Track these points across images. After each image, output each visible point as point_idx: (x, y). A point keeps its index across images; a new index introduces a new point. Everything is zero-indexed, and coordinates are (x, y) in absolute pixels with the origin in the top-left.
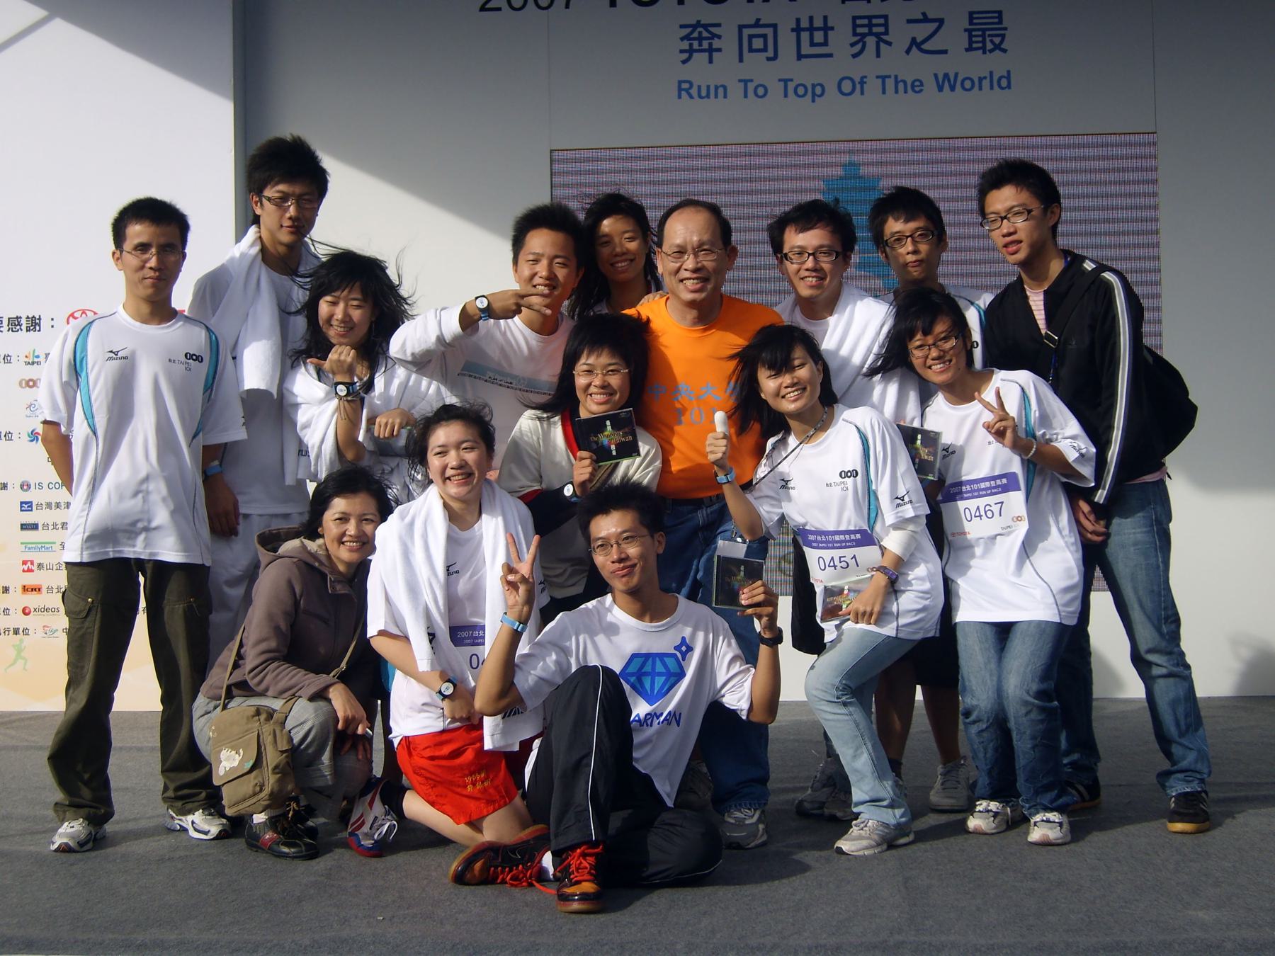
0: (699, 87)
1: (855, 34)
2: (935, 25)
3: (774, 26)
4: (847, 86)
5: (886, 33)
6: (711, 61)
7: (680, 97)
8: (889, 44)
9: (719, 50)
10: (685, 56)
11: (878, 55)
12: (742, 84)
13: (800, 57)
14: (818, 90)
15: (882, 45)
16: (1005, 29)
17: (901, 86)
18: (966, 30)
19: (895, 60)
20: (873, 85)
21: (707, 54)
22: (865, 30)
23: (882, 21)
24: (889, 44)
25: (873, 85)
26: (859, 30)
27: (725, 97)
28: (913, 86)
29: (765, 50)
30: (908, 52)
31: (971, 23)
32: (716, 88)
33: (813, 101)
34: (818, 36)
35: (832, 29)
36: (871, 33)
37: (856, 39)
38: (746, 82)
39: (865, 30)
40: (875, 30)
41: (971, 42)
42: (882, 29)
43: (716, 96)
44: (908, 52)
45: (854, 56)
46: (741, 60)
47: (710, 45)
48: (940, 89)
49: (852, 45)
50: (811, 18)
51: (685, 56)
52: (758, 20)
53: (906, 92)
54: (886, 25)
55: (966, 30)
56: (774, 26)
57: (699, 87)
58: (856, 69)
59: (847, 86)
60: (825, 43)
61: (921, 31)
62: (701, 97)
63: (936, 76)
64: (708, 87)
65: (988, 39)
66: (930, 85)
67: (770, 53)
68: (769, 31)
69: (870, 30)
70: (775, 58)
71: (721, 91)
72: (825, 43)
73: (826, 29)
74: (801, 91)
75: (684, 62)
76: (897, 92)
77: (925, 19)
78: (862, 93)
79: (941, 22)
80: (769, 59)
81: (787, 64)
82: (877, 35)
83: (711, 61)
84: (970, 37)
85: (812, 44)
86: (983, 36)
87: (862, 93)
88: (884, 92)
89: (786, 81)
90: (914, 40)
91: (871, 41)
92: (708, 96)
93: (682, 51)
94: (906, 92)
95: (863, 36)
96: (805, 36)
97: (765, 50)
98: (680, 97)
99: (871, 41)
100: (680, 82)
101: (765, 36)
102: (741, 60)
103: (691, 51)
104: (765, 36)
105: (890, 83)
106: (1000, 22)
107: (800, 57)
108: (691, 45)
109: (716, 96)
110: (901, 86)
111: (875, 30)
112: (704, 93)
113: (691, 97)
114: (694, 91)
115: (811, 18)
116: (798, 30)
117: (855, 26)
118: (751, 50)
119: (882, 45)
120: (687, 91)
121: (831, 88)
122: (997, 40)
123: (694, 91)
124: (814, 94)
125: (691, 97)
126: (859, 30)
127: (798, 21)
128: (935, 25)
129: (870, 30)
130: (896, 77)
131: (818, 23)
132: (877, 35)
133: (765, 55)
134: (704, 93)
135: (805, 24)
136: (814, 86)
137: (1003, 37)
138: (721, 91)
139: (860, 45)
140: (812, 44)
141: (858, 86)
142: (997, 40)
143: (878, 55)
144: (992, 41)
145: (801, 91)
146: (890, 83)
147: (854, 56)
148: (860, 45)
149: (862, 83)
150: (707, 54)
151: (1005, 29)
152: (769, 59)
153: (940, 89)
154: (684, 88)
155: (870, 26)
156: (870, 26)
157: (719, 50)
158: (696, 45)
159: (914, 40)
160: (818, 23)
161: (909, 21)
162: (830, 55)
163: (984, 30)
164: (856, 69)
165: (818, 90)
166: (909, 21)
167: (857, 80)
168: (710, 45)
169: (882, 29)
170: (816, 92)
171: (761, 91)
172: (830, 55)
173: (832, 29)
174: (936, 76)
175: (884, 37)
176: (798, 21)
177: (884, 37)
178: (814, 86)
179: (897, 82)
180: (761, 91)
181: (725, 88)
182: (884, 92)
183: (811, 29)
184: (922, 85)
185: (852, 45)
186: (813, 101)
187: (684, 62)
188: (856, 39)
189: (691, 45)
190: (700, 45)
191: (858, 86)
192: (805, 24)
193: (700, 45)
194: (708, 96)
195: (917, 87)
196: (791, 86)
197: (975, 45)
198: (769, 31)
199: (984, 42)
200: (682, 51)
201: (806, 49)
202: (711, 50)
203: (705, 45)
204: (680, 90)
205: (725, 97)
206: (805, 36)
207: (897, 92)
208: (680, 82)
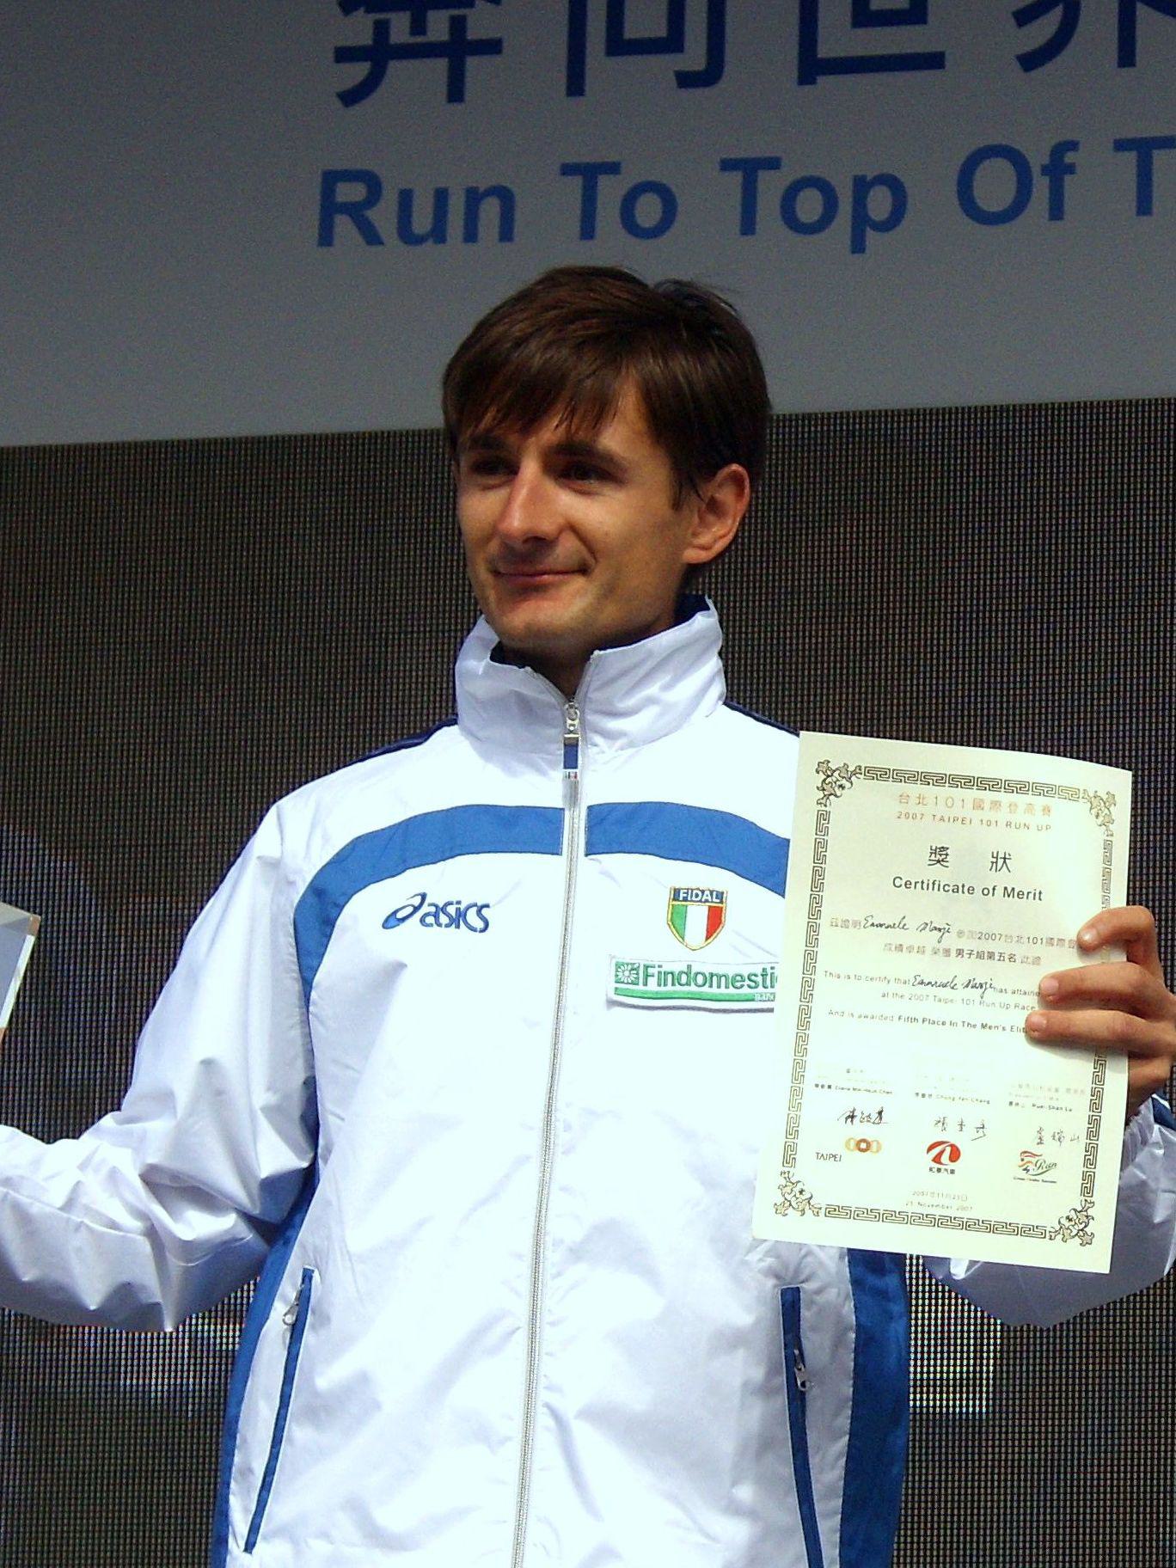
0: (406, 198)
4: (995, 185)
6: (456, 92)
7: (326, 237)
9: (492, 47)
10: (360, 70)
11: (1127, 57)
12: (577, 182)
13: (811, 67)
14: (879, 203)
20: (1102, 178)
21: (441, 65)
25: (1102, 178)
27: (506, 234)
29: (673, 42)
32: (474, 198)
33: (858, 246)
38: (590, 174)
43: (471, 235)
45: (1030, 61)
46: (576, 85)
47: (458, 25)
51: (360, 70)
57: (406, 198)
58: (1033, 115)
59: (995, 185)
62: (406, 234)
64: (441, 197)
67: (694, 57)
70: (710, 75)
71: (490, 210)
74: (809, 206)
75: (351, 97)
78: (1056, 211)
80: (686, 80)
81: (760, 98)
83: (456, 92)
87: (1056, 211)
89: (750, 169)
92: (438, 233)
93: (344, 55)
97: (673, 42)
98: (326, 237)
100: (331, 179)
102: (576, 85)
103: (379, 54)
107: (811, 67)
108: (381, 29)
109: (471, 235)
112: (422, 221)
113: (372, 237)
114: (384, 217)
118: (618, 45)
120: (356, 211)
121: (931, 193)
123: (384, 217)
124: (861, 221)
125: (372, 237)
133: (664, 66)
134: (422, 221)
136: (862, 187)
138: (490, 210)
141: (1041, 187)
143: (1127, 57)
145: (809, 206)
147: (1030, 61)
149: (1058, 169)
150: (441, 65)
152: (686, 80)
154: (345, 202)
157: (492, 47)
158: (400, 28)
162: (934, 61)
164: (1033, 115)
165: (879, 203)
167: (1037, 158)
168: (458, 25)
171: (648, 210)
172: (934, 61)
180: (648, 210)
181: (505, 197)
186: (858, 246)
187: (351, 97)
189: (381, 29)
190: (418, 27)
191: (1041, 187)
193: (418, 27)
194: (438, 233)
196: (771, 187)
200: (344, 55)
202: (458, 49)
203: (438, 26)
204: (329, 209)
205: (506, 234)
208: (331, 179)
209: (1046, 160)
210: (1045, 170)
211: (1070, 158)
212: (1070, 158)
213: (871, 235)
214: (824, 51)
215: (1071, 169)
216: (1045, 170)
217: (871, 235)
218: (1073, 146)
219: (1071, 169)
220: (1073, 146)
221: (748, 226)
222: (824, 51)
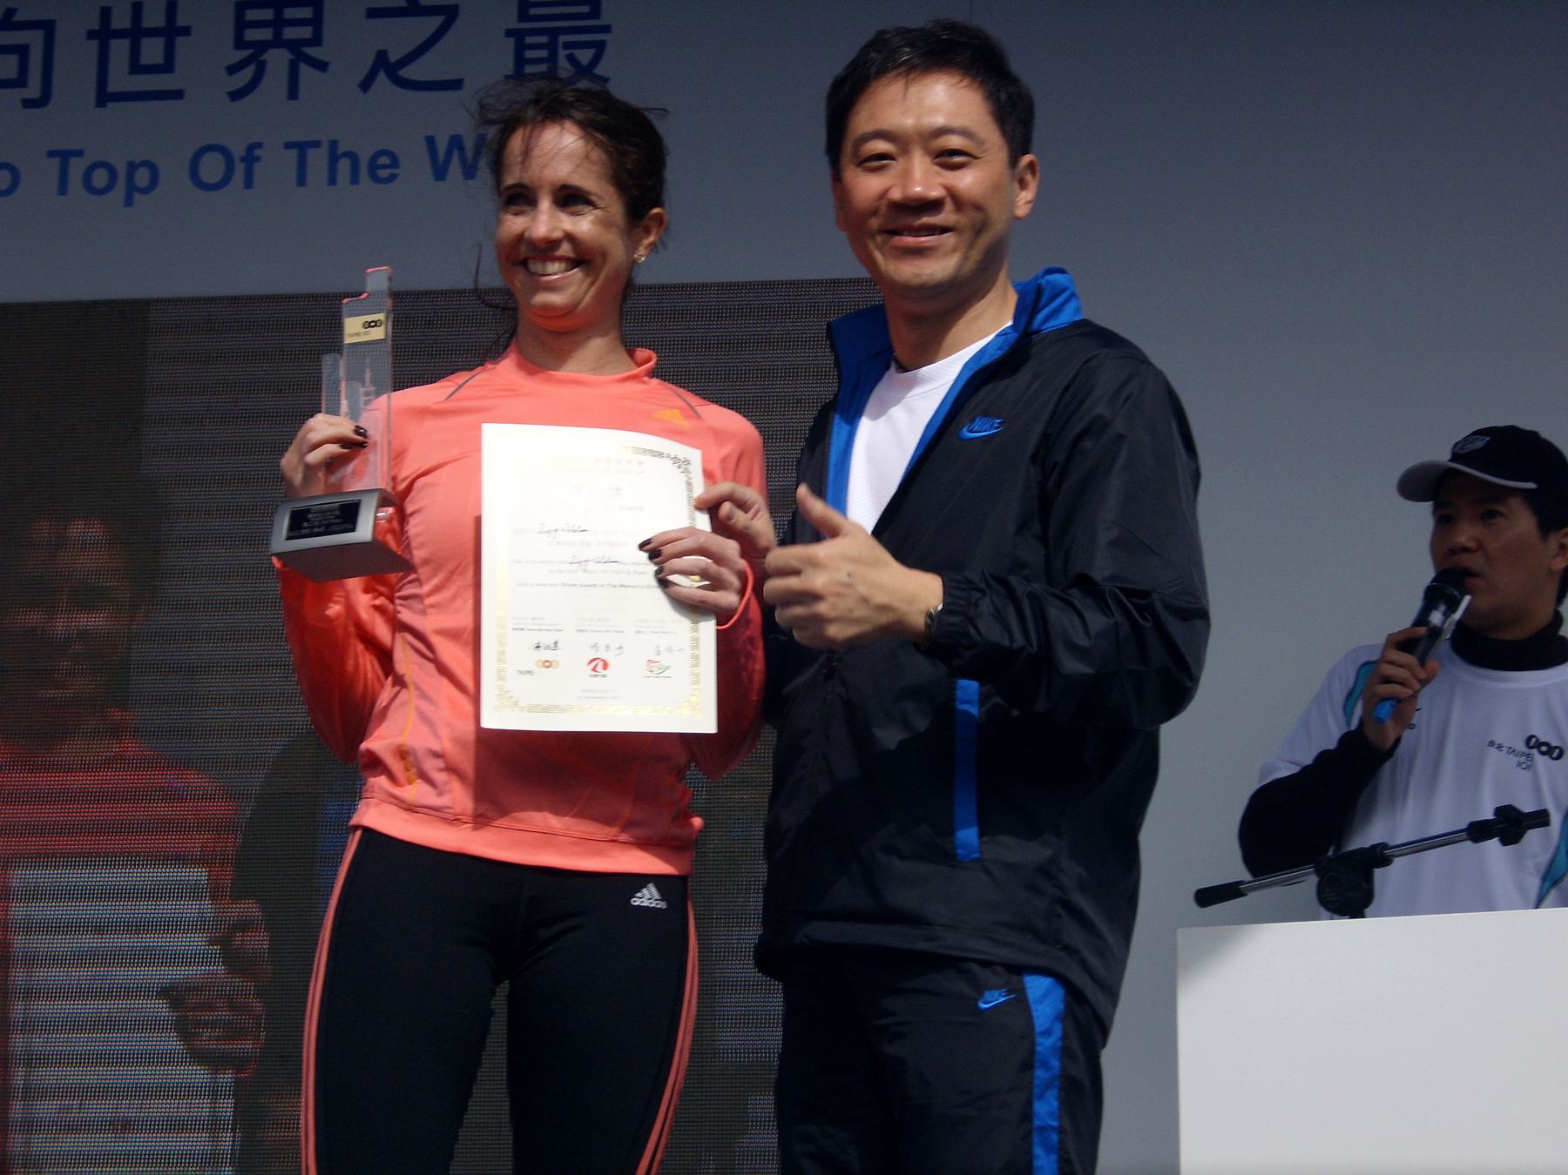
1: (240, 43)
2: (435, 22)
3: (48, 27)
4: (212, 168)
5: (317, 40)
8: (321, 66)
11: (293, 94)
13: (104, 97)
14: (142, 177)
15: (304, 69)
16: (606, 29)
17: (344, 166)
18: (509, 33)
19: (335, 105)
20: (276, 166)
22: (266, 34)
23: (306, 13)
24: (321, 66)
25: (276, 166)
26: (252, 35)
28: (373, 167)
29: (20, 81)
30: (365, 85)
31: (523, 16)
33: (129, 202)
34: (152, 51)
35: (186, 31)
36: (278, 42)
37: (245, 53)
39: (266, 34)
40: (290, 33)
41: (520, 61)
42: (305, 32)
44: (365, 85)
45: (236, 95)
48: (440, 173)
49: (232, 70)
50: (137, 10)
52: (11, 12)
53: (355, 179)
54: (316, 22)
55: (509, 33)
56: (48, 27)
59: (212, 168)
60: (167, 67)
61: (401, 36)
63: (431, 142)
65: (562, 53)
66: (416, 164)
67: (33, 90)
68: (35, 39)
69: (278, 33)
70: (43, 100)
72: (167, 67)
73: (172, 32)
74: (100, 178)
76: (332, 181)
77: (414, 9)
78: (248, 184)
79: (451, 13)
80: (28, 104)
82: (294, 46)
84: (520, 48)
85: (136, 68)
86: (552, 47)
87: (248, 184)
88: (302, 180)
89: (64, 157)
90: (381, 57)
91: (277, 60)
94: (355, 179)
95: (262, 47)
96: (119, 50)
97: (20, 81)
99: (277, 60)
101: (22, 51)
104: (22, 51)
105: (318, 160)
106: (595, 13)
107: (104, 97)
110: (344, 166)
111: (290, 33)
115: (137, 10)
116: (103, 34)
117: (241, 25)
119: (304, 69)
122: (585, 56)
124: (131, 188)
126: (252, 35)
127: (106, 13)
128: (435, 22)
129: (278, 33)
130: (333, 144)
131: (154, 17)
132: (294, 46)
135: (121, 20)
136: (132, 167)
137: (600, 47)
139: (247, 74)
140: (136, 68)
141: (240, 169)
142: (585, 56)
143: (293, 94)
144: (572, 59)
145: (100, 178)
146: (318, 160)
147: (236, 95)
148: (247, 74)
149: (250, 158)
151: (606, 29)
153: (440, 173)
155: (278, 24)
156: (278, 24)
159: (381, 57)
160: (154, 17)
161: (373, 13)
162: (178, 95)
163: (553, 33)
165: (142, 177)
166: (373, 13)
167: (238, 152)
169: (305, 32)
170: (137, 180)
172: (178, 95)
173: (186, 31)
174: (431, 142)
175: (311, 51)
176: (106, 13)
177: (311, 51)
178: (132, 167)
179: (334, 158)
182: (302, 180)
183: (136, 33)
184: (395, 163)
185: (232, 70)
186: (129, 202)
188: (245, 53)
191: (240, 169)
192: (121, 20)
195: (383, 166)
196: (77, 167)
197: (529, 69)
198: (35, 39)
199: (552, 59)
201: (120, 79)
206: (119, 50)
207: (332, 181)
209: (243, 154)
210: (243, 159)
211: (257, 152)
212: (257, 152)
213: (137, 196)
214: (114, 86)
215: (258, 159)
216: (243, 159)
217: (137, 196)
218: (259, 145)
219: (258, 159)
220: (259, 145)
221: (63, 188)
222: (114, 86)
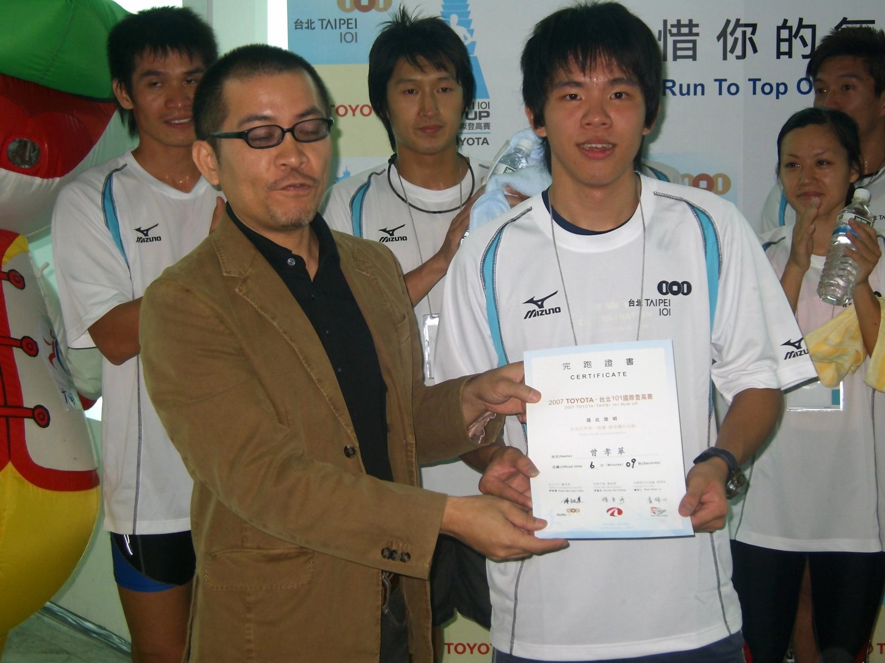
0: (681, 86)
12: (718, 83)
14: (782, 89)
27: (703, 94)
33: (778, 97)
57: (681, 86)
62: (681, 93)
64: (689, 86)
71: (699, 89)
112: (685, 91)
113: (674, 94)
123: (676, 89)
124: (778, 92)
125: (674, 94)
134: (685, 91)
136: (778, 85)
138: (699, 89)
165: (782, 89)
178: (778, 85)
181: (702, 86)
186: (778, 97)
194: (688, 93)
205: (703, 94)
